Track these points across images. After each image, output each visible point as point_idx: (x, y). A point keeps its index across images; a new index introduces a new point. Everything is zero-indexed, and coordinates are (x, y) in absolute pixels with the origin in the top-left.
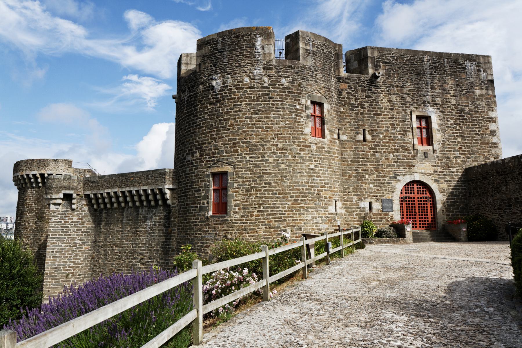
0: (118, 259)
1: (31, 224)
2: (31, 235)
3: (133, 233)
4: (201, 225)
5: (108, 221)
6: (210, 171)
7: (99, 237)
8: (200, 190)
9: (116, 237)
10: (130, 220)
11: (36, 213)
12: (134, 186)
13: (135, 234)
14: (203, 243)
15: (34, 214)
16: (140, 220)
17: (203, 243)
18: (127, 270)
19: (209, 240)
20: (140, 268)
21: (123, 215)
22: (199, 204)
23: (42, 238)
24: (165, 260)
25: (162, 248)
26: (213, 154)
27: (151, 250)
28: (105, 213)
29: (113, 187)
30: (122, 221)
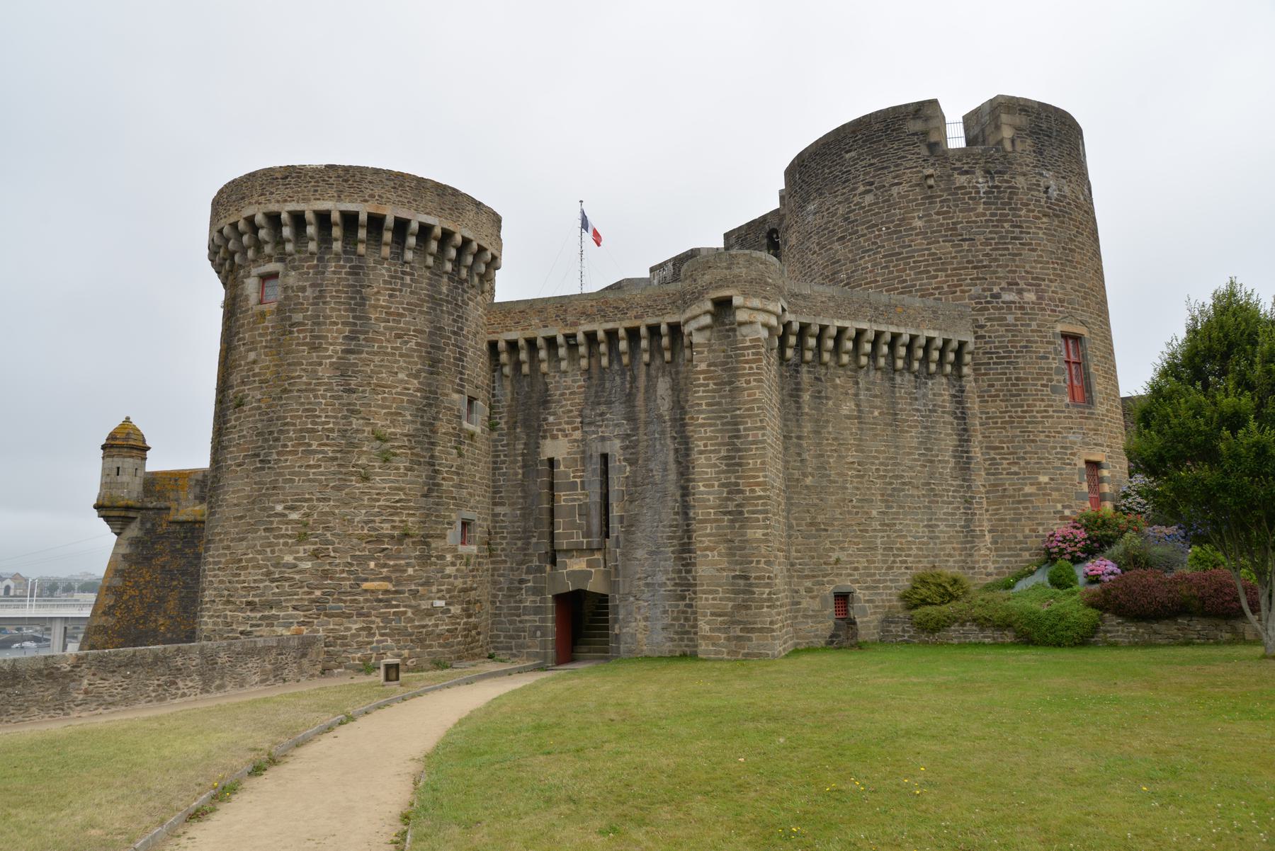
0: (858, 476)
1: (401, 376)
2: (405, 409)
3: (886, 424)
4: (1059, 417)
5: (820, 392)
6: (1059, 328)
7: (799, 426)
8: (1047, 358)
9: (845, 429)
10: (876, 396)
11: (418, 344)
12: (906, 325)
13: (891, 425)
14: (1066, 448)
15: (412, 344)
16: (901, 398)
17: (1066, 448)
18: (882, 501)
19: (1075, 443)
20: (912, 496)
21: (857, 383)
22: (1051, 380)
23: (438, 423)
24: (964, 480)
25: (955, 457)
26: (1061, 301)
27: (931, 462)
28: (809, 372)
29: (854, 316)
30: (857, 395)
